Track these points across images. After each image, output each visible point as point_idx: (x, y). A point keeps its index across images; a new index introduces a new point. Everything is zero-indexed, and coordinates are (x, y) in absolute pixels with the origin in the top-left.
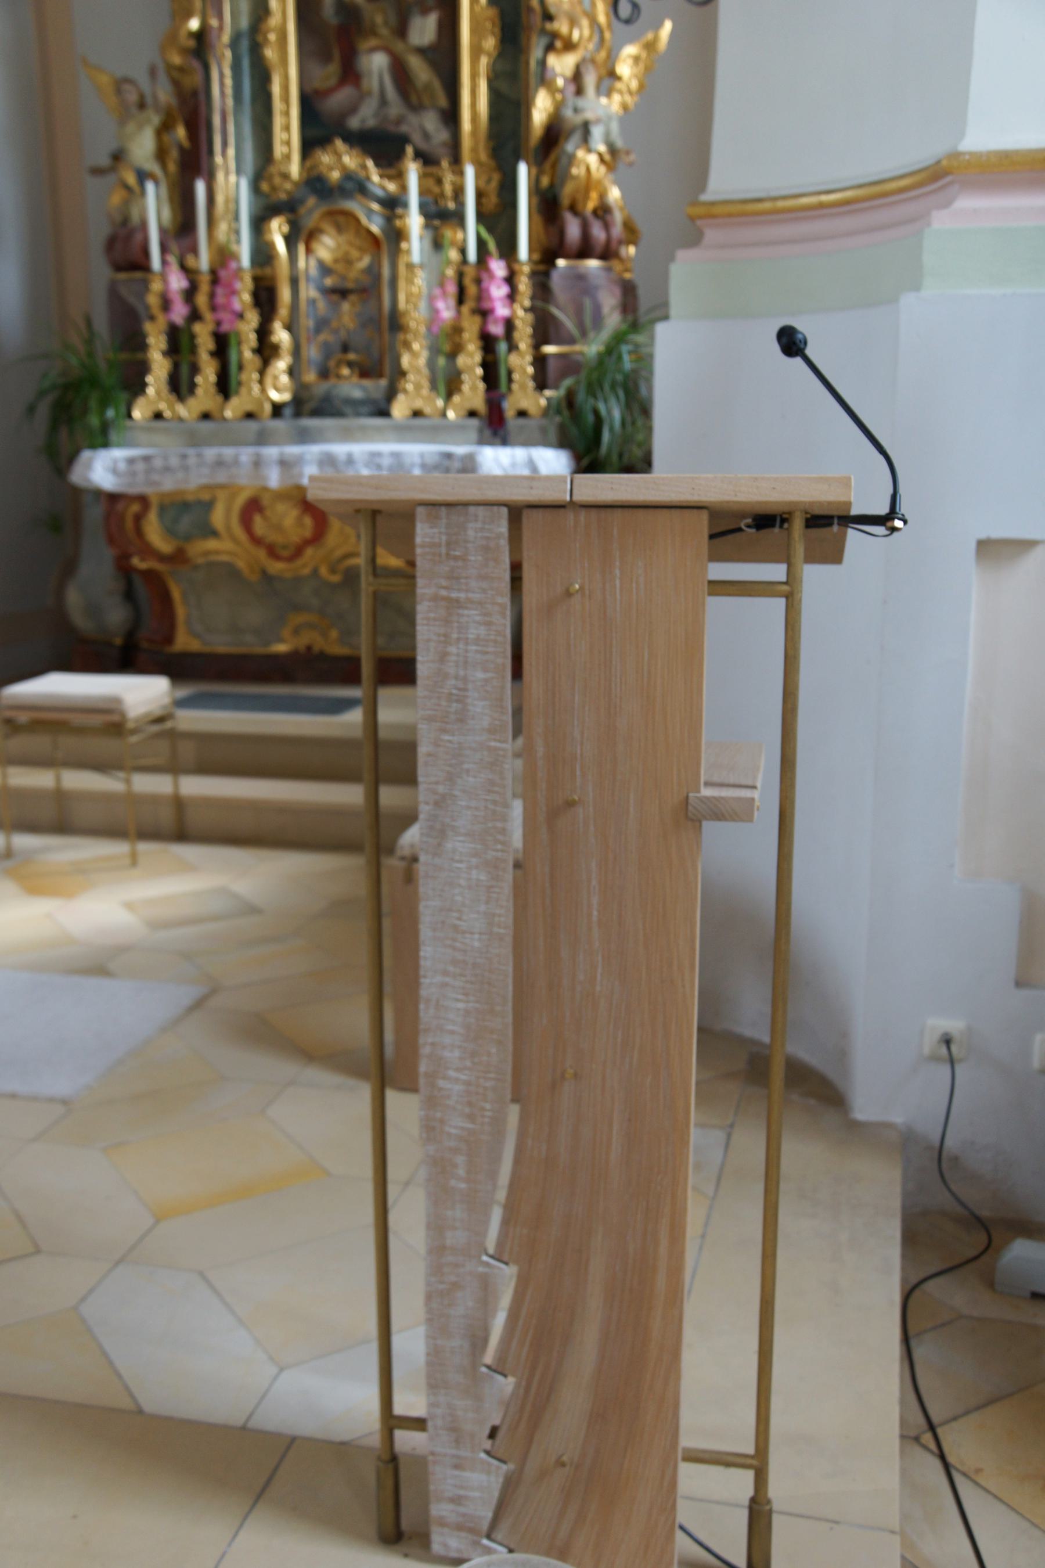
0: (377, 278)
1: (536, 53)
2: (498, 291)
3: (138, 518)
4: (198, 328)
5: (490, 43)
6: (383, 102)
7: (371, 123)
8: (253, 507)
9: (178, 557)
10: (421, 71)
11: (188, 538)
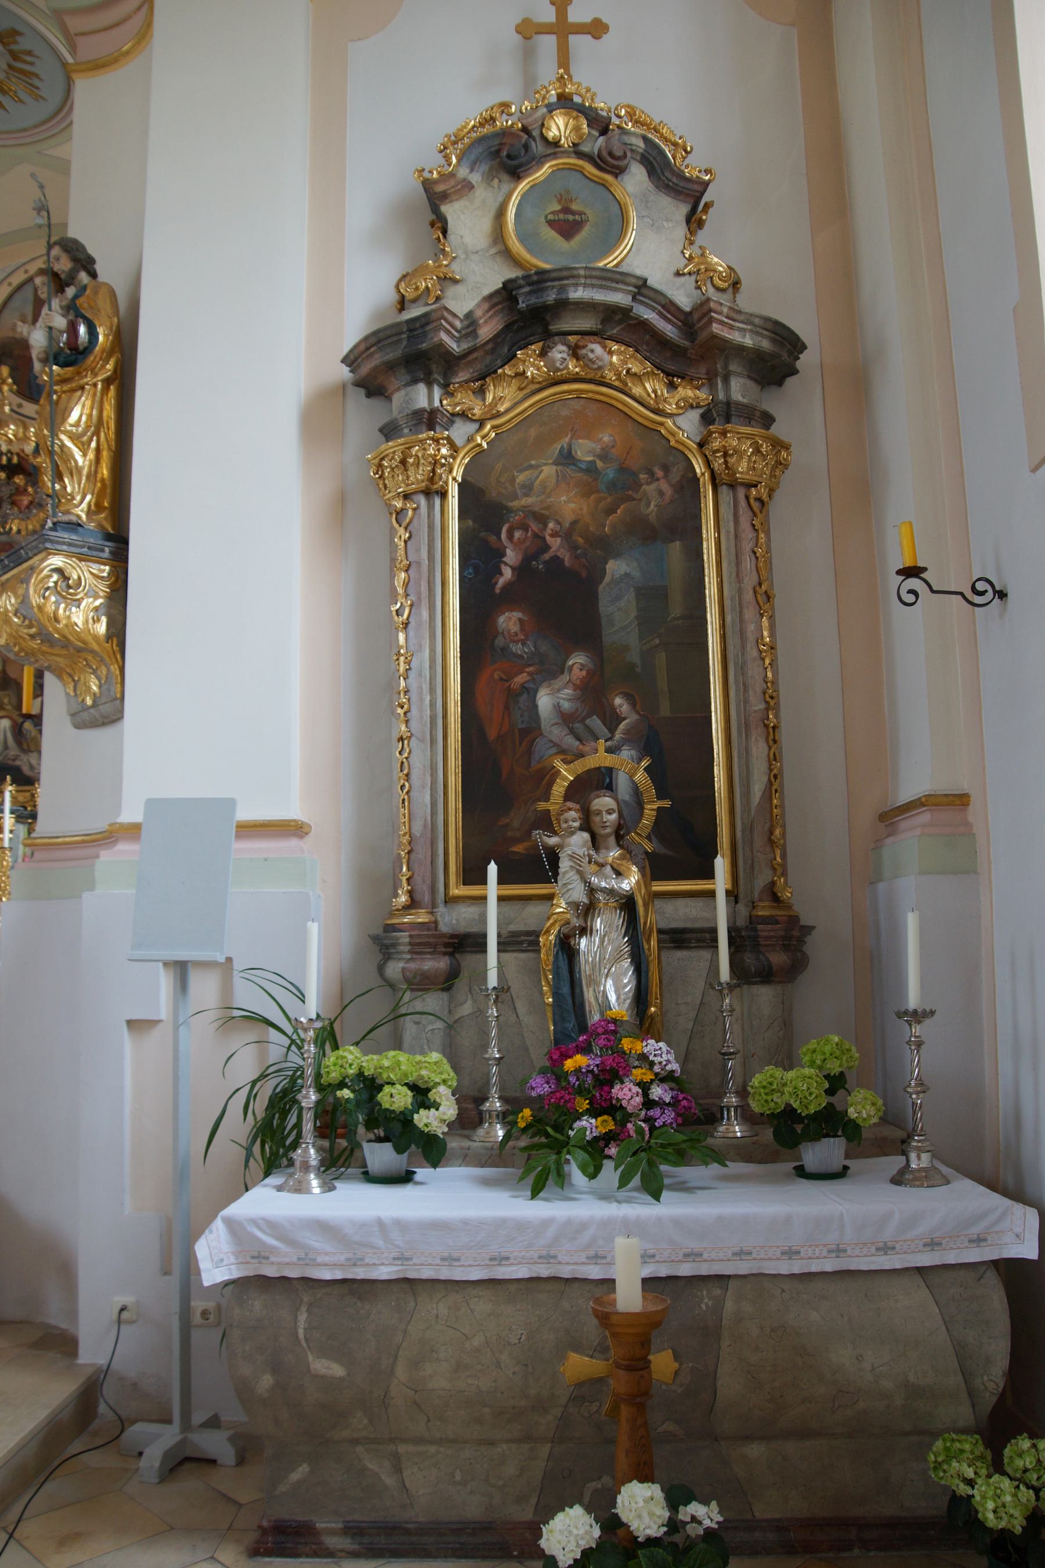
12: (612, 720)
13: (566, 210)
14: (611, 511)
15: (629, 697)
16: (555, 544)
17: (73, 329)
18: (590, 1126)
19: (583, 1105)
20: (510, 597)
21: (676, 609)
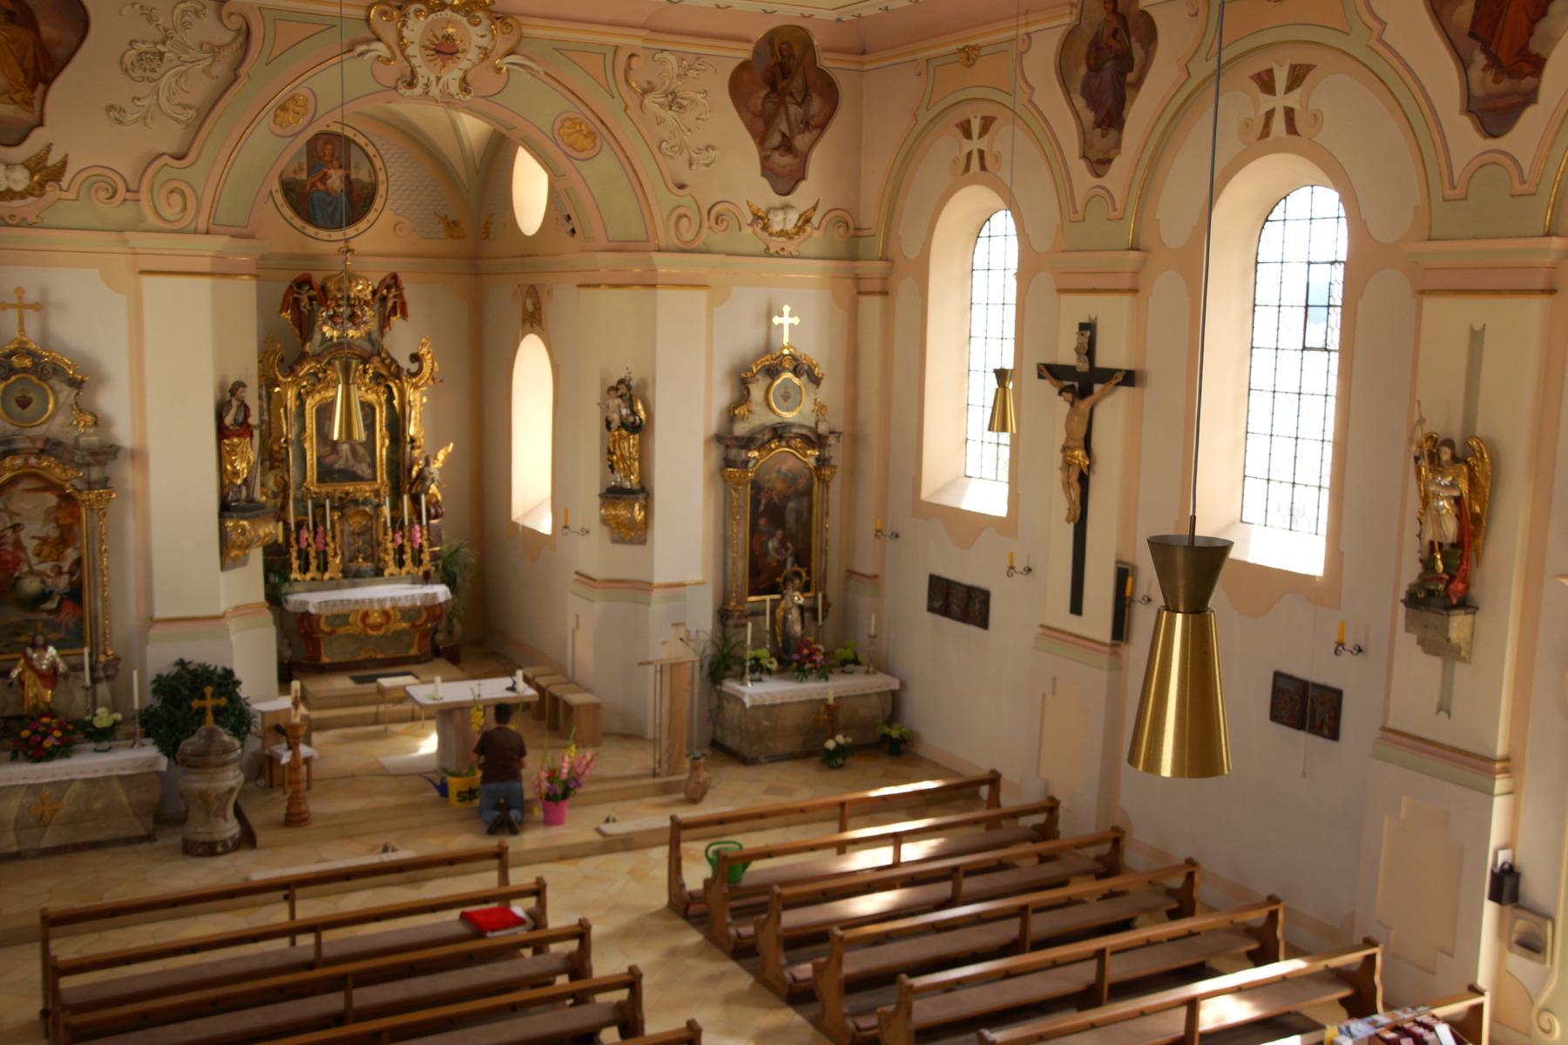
0: (372, 528)
1: (408, 448)
2: (418, 535)
3: (318, 621)
4: (309, 549)
5: (387, 442)
6: (347, 460)
7: (343, 467)
8: (366, 615)
9: (333, 632)
10: (361, 450)
11: (338, 626)
12: (787, 549)
13: (786, 392)
14: (790, 487)
15: (792, 542)
16: (775, 498)
17: (635, 420)
18: (808, 666)
19: (807, 661)
20: (763, 514)
21: (805, 515)
